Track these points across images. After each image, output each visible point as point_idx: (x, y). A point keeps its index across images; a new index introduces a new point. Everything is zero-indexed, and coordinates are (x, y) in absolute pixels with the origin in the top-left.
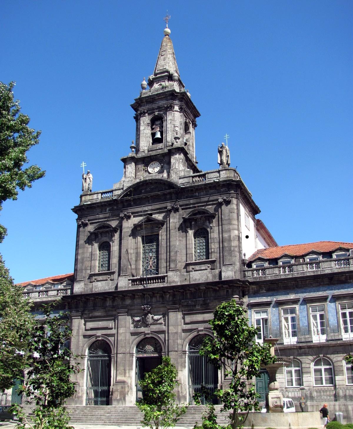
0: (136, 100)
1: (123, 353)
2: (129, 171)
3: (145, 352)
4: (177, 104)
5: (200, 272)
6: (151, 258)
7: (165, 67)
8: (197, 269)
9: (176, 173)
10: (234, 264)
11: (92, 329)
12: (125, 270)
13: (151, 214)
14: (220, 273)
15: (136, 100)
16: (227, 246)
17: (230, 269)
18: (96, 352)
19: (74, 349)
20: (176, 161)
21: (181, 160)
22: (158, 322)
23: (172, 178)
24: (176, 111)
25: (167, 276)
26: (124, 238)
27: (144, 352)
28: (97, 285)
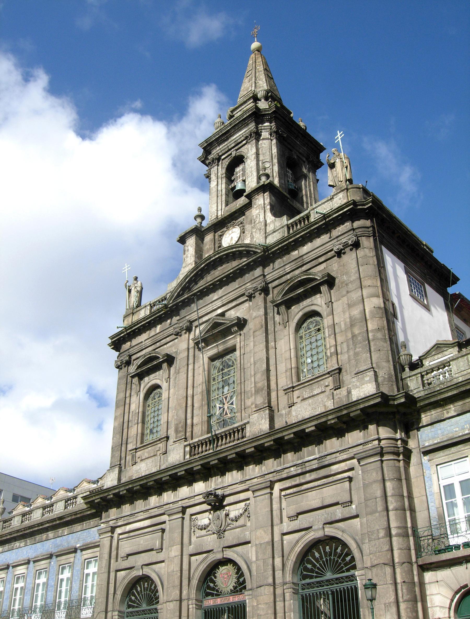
0: (201, 145)
1: (176, 599)
2: (189, 255)
3: (219, 595)
4: (264, 129)
5: (310, 401)
6: (226, 398)
7: (250, 90)
8: (306, 396)
9: (261, 229)
10: (378, 367)
12: (180, 429)
13: (223, 314)
14: (349, 392)
16: (359, 333)
17: (367, 379)
18: (137, 604)
20: (261, 211)
21: (269, 207)
22: (238, 523)
23: (255, 240)
24: (263, 139)
25: (248, 423)
26: (181, 370)
27: (217, 595)
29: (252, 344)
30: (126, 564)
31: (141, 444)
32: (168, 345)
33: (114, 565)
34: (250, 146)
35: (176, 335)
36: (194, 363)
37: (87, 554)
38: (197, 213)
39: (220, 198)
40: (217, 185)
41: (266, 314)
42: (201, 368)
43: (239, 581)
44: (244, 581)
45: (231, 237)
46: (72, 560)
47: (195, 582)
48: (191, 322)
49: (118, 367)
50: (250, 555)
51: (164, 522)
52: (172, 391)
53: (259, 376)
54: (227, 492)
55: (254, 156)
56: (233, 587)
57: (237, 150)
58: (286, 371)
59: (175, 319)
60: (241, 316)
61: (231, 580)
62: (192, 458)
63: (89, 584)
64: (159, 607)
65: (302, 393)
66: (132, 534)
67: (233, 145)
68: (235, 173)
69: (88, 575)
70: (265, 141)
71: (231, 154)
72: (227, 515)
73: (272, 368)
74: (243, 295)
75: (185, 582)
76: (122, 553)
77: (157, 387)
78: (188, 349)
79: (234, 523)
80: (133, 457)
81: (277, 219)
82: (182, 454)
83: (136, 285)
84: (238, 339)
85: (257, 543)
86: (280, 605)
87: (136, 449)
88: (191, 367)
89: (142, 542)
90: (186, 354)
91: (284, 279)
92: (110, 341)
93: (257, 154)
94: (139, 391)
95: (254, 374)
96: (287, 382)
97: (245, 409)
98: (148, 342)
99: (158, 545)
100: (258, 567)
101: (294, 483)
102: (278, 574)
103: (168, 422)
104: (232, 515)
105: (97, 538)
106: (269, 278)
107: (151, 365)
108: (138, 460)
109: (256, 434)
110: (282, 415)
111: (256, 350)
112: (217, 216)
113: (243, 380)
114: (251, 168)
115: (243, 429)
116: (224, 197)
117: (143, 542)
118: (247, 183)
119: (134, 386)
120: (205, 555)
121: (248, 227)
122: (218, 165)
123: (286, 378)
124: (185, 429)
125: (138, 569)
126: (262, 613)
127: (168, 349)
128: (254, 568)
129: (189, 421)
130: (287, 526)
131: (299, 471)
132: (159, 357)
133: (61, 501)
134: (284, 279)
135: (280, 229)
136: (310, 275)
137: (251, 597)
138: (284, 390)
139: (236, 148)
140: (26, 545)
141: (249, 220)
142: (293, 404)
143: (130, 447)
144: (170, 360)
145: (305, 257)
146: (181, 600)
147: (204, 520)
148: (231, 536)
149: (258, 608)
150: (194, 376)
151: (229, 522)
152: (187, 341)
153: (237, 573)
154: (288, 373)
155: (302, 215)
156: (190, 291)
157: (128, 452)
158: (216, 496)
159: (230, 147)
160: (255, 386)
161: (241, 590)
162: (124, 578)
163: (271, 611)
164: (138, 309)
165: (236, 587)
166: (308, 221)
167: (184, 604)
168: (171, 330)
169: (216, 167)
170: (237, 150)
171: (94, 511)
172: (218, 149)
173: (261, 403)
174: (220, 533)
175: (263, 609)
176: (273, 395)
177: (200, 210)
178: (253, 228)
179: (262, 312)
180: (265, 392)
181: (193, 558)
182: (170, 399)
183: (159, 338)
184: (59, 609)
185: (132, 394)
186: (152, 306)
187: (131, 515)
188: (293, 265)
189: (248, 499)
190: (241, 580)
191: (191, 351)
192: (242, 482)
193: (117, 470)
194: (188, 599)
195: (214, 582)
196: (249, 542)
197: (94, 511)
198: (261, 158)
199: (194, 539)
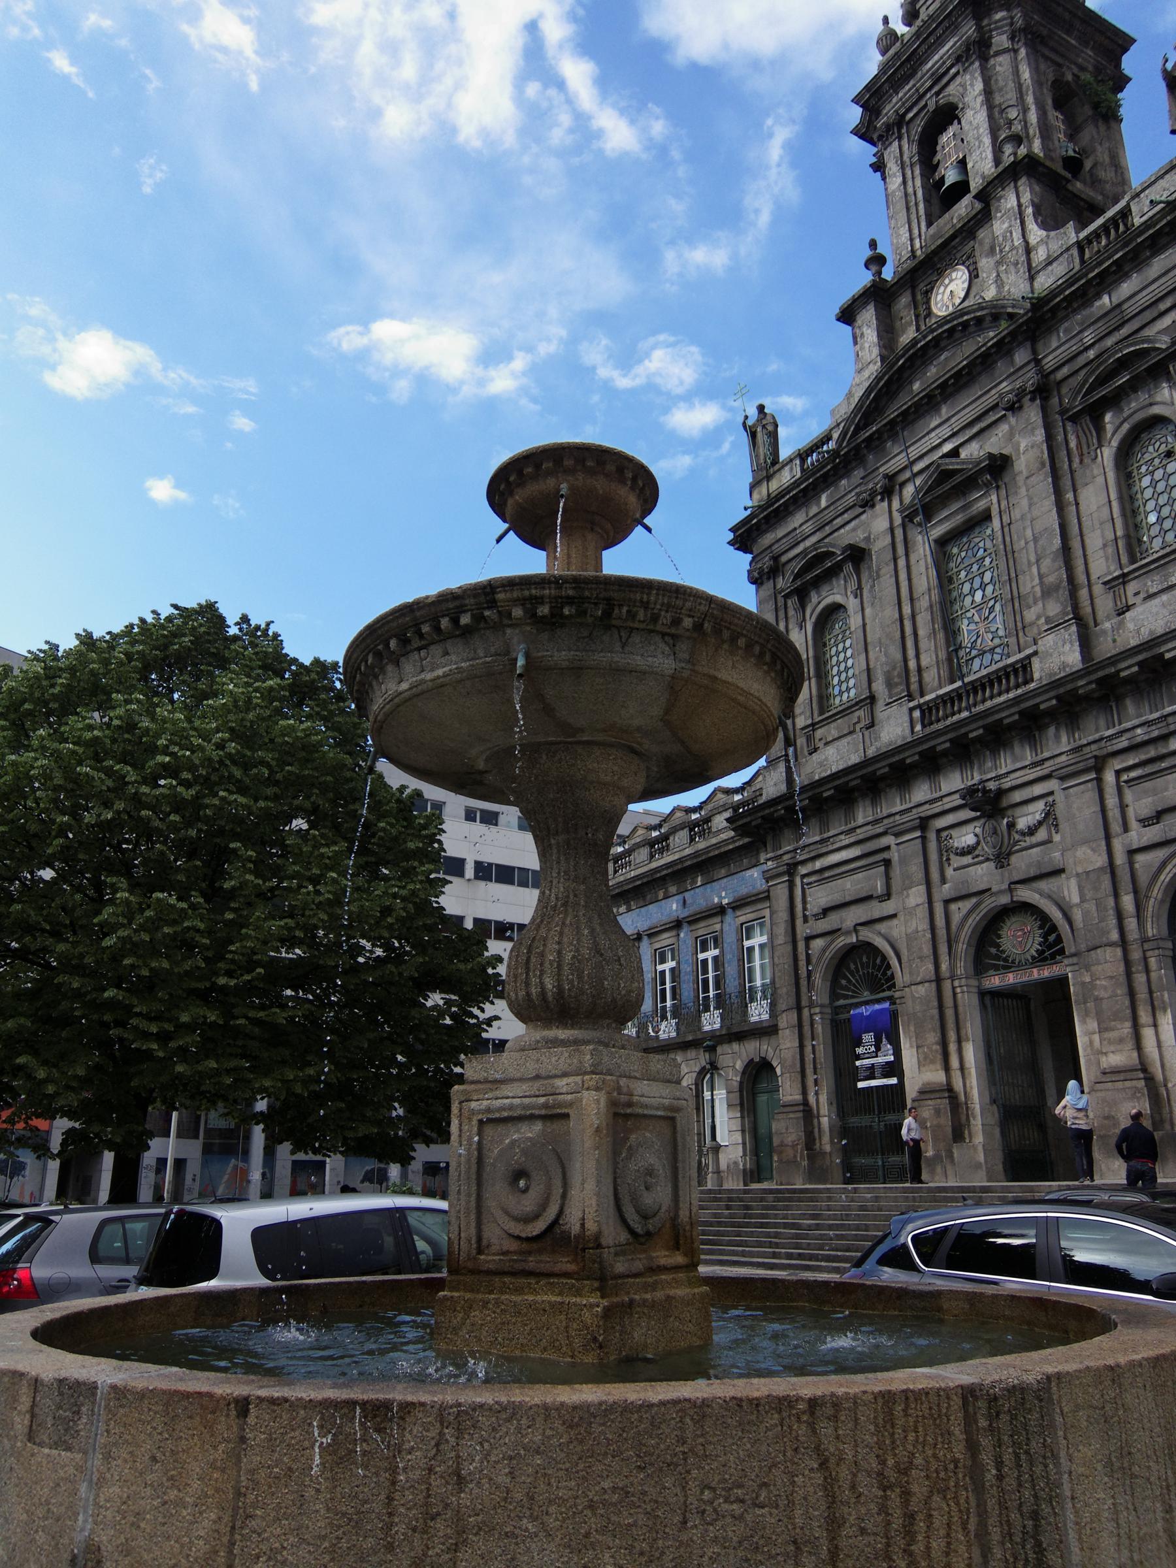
0: (856, 100)
1: (928, 978)
2: (867, 345)
4: (996, 29)
5: (1164, 597)
8: (1152, 590)
11: (826, 911)
12: (896, 680)
13: (955, 453)
15: (856, 100)
18: (854, 991)
19: (784, 990)
21: (1030, 210)
25: (1035, 653)
26: (882, 572)
27: (1005, 968)
28: (826, 759)
29: (1025, 503)
30: (823, 925)
31: (821, 714)
32: (848, 528)
33: (802, 930)
34: (968, 77)
35: (862, 507)
36: (907, 555)
37: (745, 915)
38: (868, 253)
39: (913, 210)
40: (904, 182)
41: (1049, 438)
42: (922, 563)
43: (1046, 940)
44: (1059, 939)
45: (951, 292)
46: (718, 927)
47: (961, 947)
48: (891, 478)
49: (754, 581)
50: (1066, 893)
51: (888, 848)
52: (868, 611)
53: (1046, 563)
54: (1007, 783)
55: (980, 99)
56: (1037, 951)
57: (937, 94)
58: (1105, 545)
59: (858, 473)
60: (995, 451)
61: (1031, 940)
62: (928, 730)
63: (757, 963)
64: (897, 994)
65: (1145, 585)
66: (827, 875)
67: (928, 84)
68: (939, 148)
69: (751, 949)
70: (1000, 59)
71: (926, 105)
72: (1011, 826)
73: (1076, 544)
74: (995, 407)
75: (943, 949)
76: (814, 906)
77: (835, 609)
78: (892, 529)
79: (1027, 839)
80: (809, 739)
81: (1053, 234)
82: (907, 725)
83: (764, 422)
84: (994, 498)
85: (1080, 870)
86: (1140, 979)
87: (813, 725)
88: (902, 562)
89: (848, 886)
90: (888, 540)
91: (1081, 360)
92: (731, 536)
93: (988, 92)
94: (804, 620)
95: (1037, 561)
96: (1108, 567)
97: (1024, 628)
98: (808, 528)
99: (880, 888)
100: (1086, 914)
101: (1143, 757)
102: (1131, 924)
103: (868, 669)
104: (1022, 823)
105: (761, 885)
106: (1049, 362)
107: (820, 569)
108: (820, 745)
109: (1055, 674)
110: (1104, 632)
111: (1036, 513)
112: (913, 251)
113: (1013, 575)
114: (977, 128)
115: (1024, 667)
116: (921, 206)
117: (850, 886)
118: (969, 166)
119: (791, 612)
120: (974, 900)
121: (985, 264)
122: (900, 138)
123: (1107, 559)
124: (906, 682)
125: (848, 933)
126: (1103, 994)
127: (849, 535)
128: (1077, 916)
129: (912, 664)
130: (1138, 836)
131: (1156, 734)
132: (833, 553)
133: (682, 829)
134: (1081, 360)
135: (1062, 254)
136: (1143, 342)
137: (1076, 967)
138: (1105, 583)
139: (936, 89)
140: (629, 910)
141: (987, 247)
142: (1128, 608)
143: (801, 722)
144: (857, 555)
145: (1125, 306)
146: (938, 980)
147: (965, 838)
148: (1021, 864)
149: (1094, 987)
150: (910, 580)
151: (1017, 837)
152: (887, 515)
153: (1041, 927)
154: (1110, 550)
155: (1110, 213)
156: (879, 418)
157: (798, 732)
158: (985, 791)
159: (921, 91)
160: (1041, 583)
161: (1053, 956)
162: (824, 950)
163: (1122, 991)
164: (777, 467)
165: (1043, 952)
166: (1125, 225)
167: (947, 985)
168: (851, 499)
169: (896, 143)
170: (937, 94)
171: (747, 840)
172: (894, 100)
173: (1057, 615)
174: (1002, 859)
175: (1105, 988)
176: (1083, 593)
177: (873, 244)
178: (998, 263)
179: (1040, 435)
180: (1064, 594)
181: (953, 907)
182: (868, 628)
183: (828, 518)
184: (707, 1009)
185: (790, 627)
186: (803, 455)
187: (822, 841)
188: (1101, 328)
189: (1052, 793)
190: (1052, 938)
191: (899, 533)
192: (1034, 765)
193: (782, 767)
194: (952, 978)
195: (998, 946)
196: (1059, 872)
197: (747, 840)
198: (998, 99)
199: (949, 872)
